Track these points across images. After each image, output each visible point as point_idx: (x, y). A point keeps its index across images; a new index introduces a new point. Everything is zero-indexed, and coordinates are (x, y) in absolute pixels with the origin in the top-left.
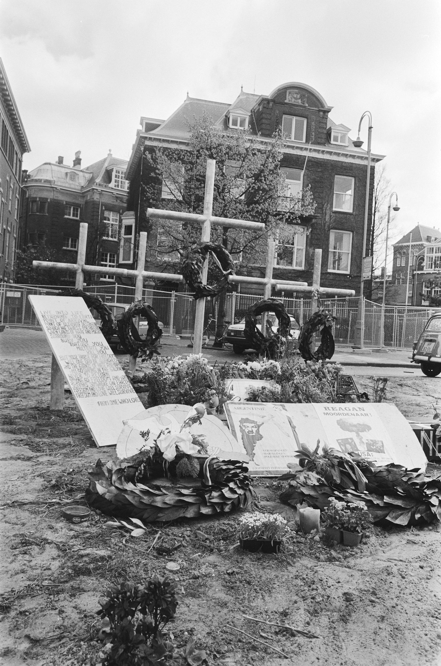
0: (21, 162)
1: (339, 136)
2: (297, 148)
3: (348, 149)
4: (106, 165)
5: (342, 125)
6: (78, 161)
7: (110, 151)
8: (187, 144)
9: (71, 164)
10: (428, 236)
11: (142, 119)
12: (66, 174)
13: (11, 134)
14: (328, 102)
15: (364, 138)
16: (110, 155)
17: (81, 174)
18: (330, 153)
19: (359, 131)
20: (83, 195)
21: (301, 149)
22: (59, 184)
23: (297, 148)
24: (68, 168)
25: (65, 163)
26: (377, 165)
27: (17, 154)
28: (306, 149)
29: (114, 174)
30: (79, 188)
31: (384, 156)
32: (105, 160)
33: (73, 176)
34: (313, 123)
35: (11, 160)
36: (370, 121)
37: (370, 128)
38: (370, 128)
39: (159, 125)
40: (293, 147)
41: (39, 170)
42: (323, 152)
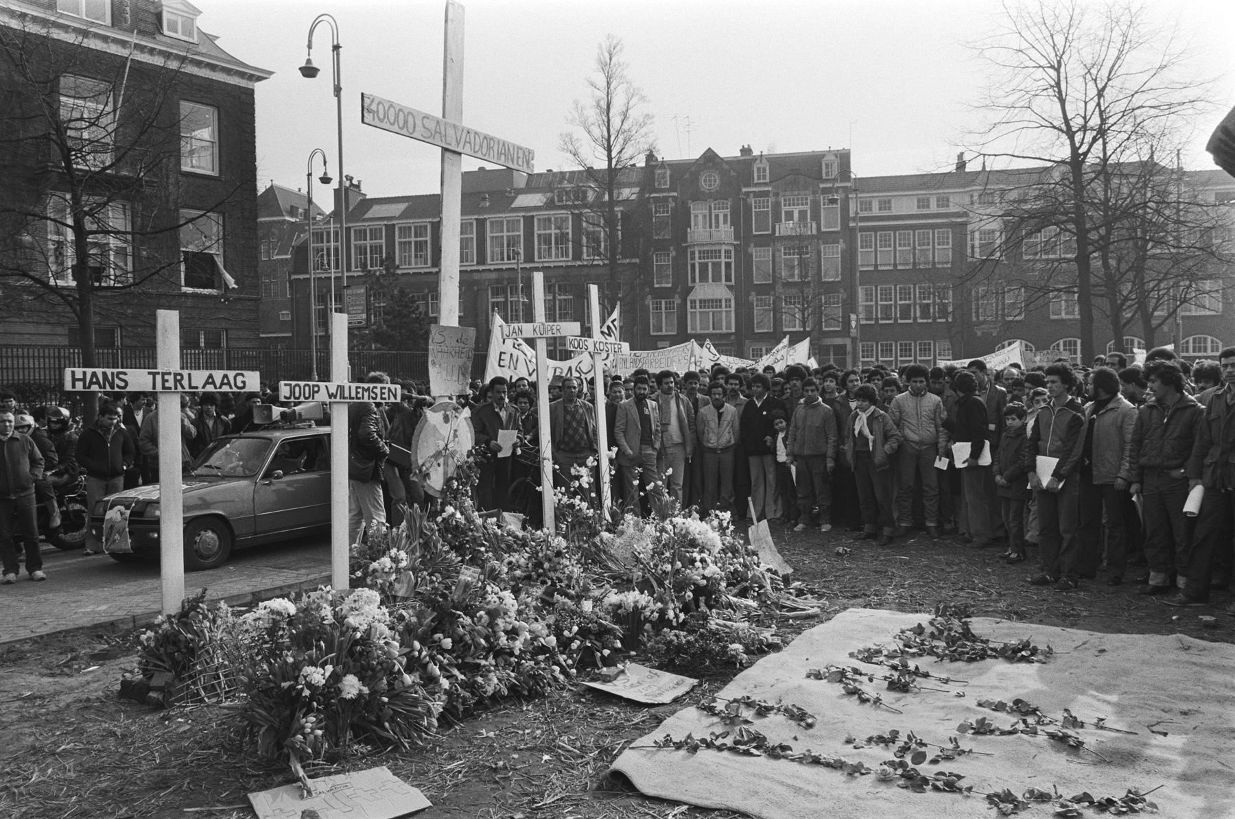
10: (292, 207)
15: (323, 60)
19: (310, 47)
26: (259, 87)
31: (271, 73)
36: (336, 33)
37: (336, 48)
38: (336, 48)
42: (152, 51)
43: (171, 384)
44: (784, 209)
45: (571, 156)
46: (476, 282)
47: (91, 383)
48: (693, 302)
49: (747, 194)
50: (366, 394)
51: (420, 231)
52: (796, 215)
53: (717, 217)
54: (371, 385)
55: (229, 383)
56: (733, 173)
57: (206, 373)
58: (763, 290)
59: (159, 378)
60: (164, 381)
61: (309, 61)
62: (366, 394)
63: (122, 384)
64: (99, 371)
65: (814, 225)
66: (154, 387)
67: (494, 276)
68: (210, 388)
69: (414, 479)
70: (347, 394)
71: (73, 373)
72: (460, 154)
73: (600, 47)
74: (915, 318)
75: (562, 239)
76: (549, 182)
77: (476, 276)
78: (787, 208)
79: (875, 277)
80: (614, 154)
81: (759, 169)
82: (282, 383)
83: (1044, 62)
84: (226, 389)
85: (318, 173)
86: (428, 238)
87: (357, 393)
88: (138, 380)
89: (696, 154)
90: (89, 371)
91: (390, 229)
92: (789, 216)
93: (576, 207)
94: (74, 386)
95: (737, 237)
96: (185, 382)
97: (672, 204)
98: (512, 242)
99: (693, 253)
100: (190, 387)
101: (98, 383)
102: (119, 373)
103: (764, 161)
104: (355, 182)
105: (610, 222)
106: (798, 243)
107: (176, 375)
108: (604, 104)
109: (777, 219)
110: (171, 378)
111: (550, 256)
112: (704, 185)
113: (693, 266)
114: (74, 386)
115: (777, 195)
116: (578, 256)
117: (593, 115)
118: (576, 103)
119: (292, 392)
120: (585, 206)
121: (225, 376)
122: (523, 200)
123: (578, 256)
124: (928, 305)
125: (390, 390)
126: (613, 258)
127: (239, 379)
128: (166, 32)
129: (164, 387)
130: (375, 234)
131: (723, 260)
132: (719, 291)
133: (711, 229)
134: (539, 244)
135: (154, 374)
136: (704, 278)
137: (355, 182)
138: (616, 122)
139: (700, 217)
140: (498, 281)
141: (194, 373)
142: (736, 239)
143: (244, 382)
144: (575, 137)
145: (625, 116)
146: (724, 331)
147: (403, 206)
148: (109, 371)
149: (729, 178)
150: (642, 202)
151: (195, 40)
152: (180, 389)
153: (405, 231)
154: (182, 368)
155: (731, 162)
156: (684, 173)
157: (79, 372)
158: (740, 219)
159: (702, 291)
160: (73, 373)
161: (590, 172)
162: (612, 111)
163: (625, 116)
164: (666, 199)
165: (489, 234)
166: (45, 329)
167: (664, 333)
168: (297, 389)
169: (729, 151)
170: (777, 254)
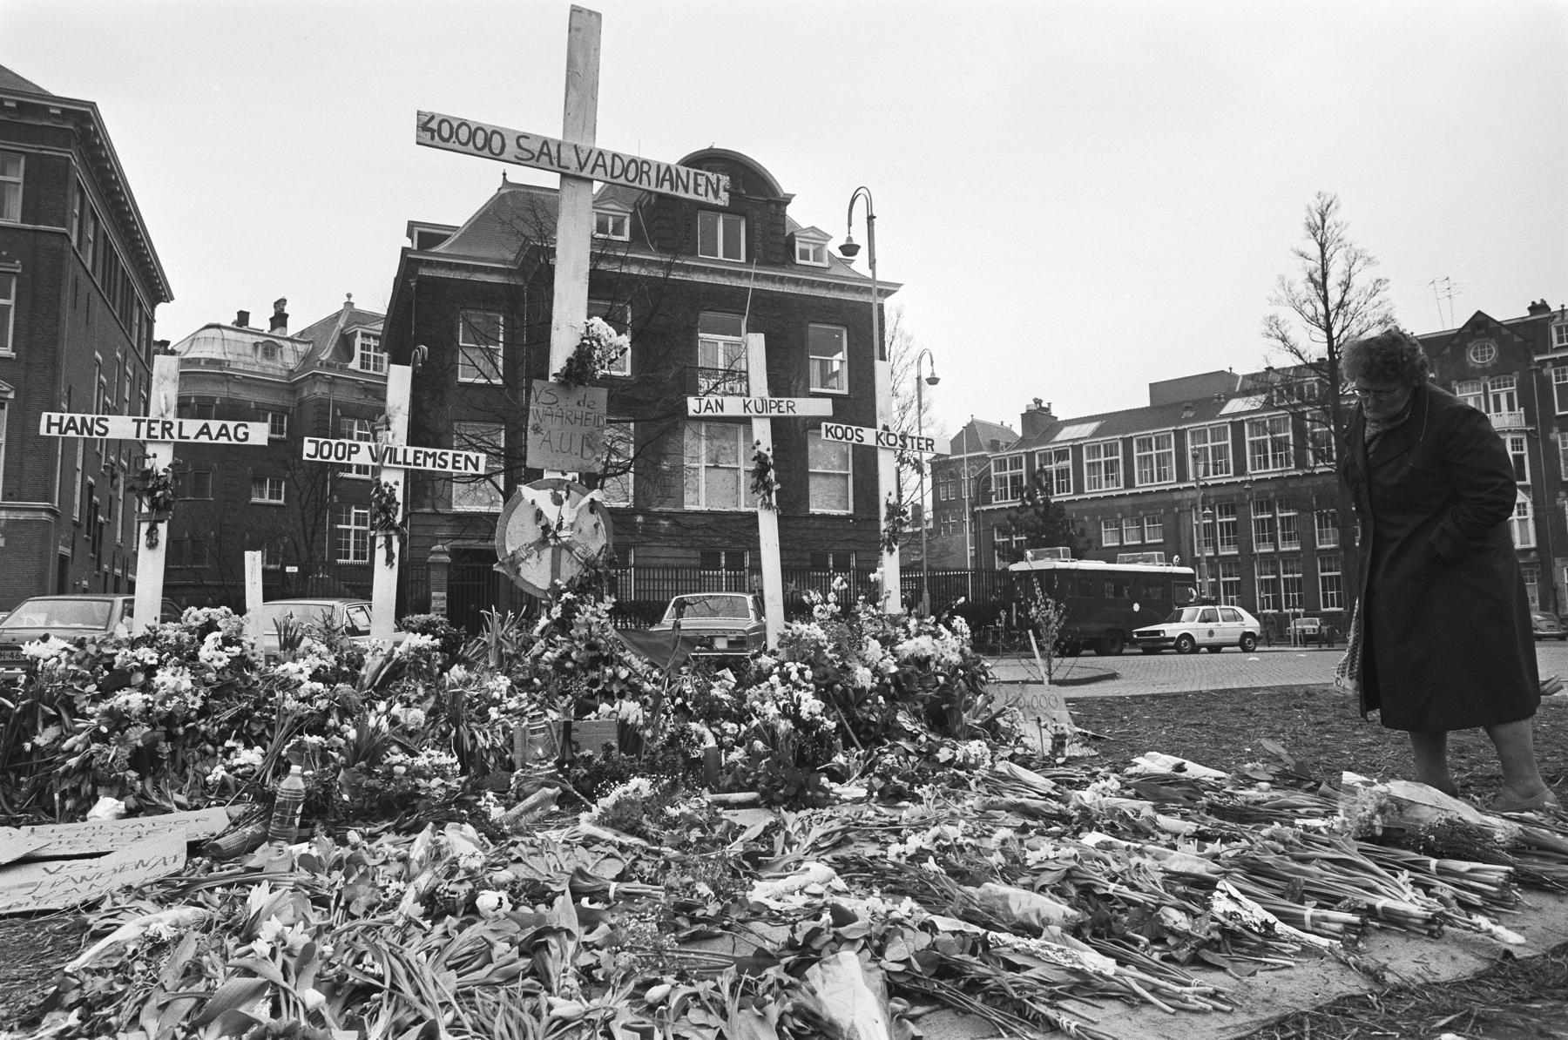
0: (150, 322)
1: (811, 248)
2: (731, 273)
3: (831, 272)
4: (341, 324)
5: (813, 229)
6: (280, 319)
7: (349, 296)
8: (509, 273)
9: (267, 327)
11: (412, 225)
12: (256, 345)
13: (123, 261)
14: (785, 185)
15: (860, 238)
16: (349, 304)
17: (287, 345)
18: (797, 282)
20: (293, 388)
21: (739, 275)
22: (241, 366)
23: (731, 273)
24: (259, 333)
25: (253, 323)
26: (888, 303)
27: (140, 305)
28: (748, 275)
29: (358, 341)
30: (284, 373)
31: (899, 285)
32: (338, 315)
33: (269, 349)
34: (758, 226)
35: (127, 317)
37: (871, 218)
38: (871, 218)
39: (447, 237)
40: (722, 273)
41: (193, 339)
42: (782, 280)
43: (157, 431)
45: (1280, 343)
46: (1177, 503)
47: (68, 428)
50: (430, 461)
51: (1111, 450)
53: (1497, 398)
54: (439, 451)
56: (1517, 339)
57: (201, 423)
59: (144, 426)
60: (150, 429)
61: (850, 239)
62: (430, 461)
64: (78, 417)
68: (204, 439)
69: (500, 569)
70: (400, 458)
72: (591, 181)
73: (1309, 209)
77: (1177, 496)
80: (1335, 333)
84: (223, 440)
85: (926, 375)
86: (1120, 457)
87: (416, 458)
88: (121, 427)
89: (1456, 320)
90: (67, 416)
91: (1077, 450)
93: (1295, 406)
95: (1529, 421)
96: (175, 432)
100: (180, 436)
101: (75, 428)
104: (1044, 405)
107: (164, 423)
108: (1318, 276)
110: (158, 427)
111: (1267, 466)
112: (1473, 360)
117: (1305, 290)
118: (1282, 279)
119: (319, 450)
121: (224, 426)
122: (1235, 405)
125: (467, 458)
128: (798, 261)
129: (149, 435)
130: (1062, 455)
134: (1252, 453)
135: (139, 422)
137: (1044, 405)
138: (1335, 296)
142: (1528, 423)
143: (246, 434)
144: (1281, 319)
145: (1346, 285)
147: (1095, 425)
148: (88, 417)
151: (825, 264)
152: (167, 438)
153: (1094, 450)
157: (55, 417)
166: (679, 552)
168: (326, 447)
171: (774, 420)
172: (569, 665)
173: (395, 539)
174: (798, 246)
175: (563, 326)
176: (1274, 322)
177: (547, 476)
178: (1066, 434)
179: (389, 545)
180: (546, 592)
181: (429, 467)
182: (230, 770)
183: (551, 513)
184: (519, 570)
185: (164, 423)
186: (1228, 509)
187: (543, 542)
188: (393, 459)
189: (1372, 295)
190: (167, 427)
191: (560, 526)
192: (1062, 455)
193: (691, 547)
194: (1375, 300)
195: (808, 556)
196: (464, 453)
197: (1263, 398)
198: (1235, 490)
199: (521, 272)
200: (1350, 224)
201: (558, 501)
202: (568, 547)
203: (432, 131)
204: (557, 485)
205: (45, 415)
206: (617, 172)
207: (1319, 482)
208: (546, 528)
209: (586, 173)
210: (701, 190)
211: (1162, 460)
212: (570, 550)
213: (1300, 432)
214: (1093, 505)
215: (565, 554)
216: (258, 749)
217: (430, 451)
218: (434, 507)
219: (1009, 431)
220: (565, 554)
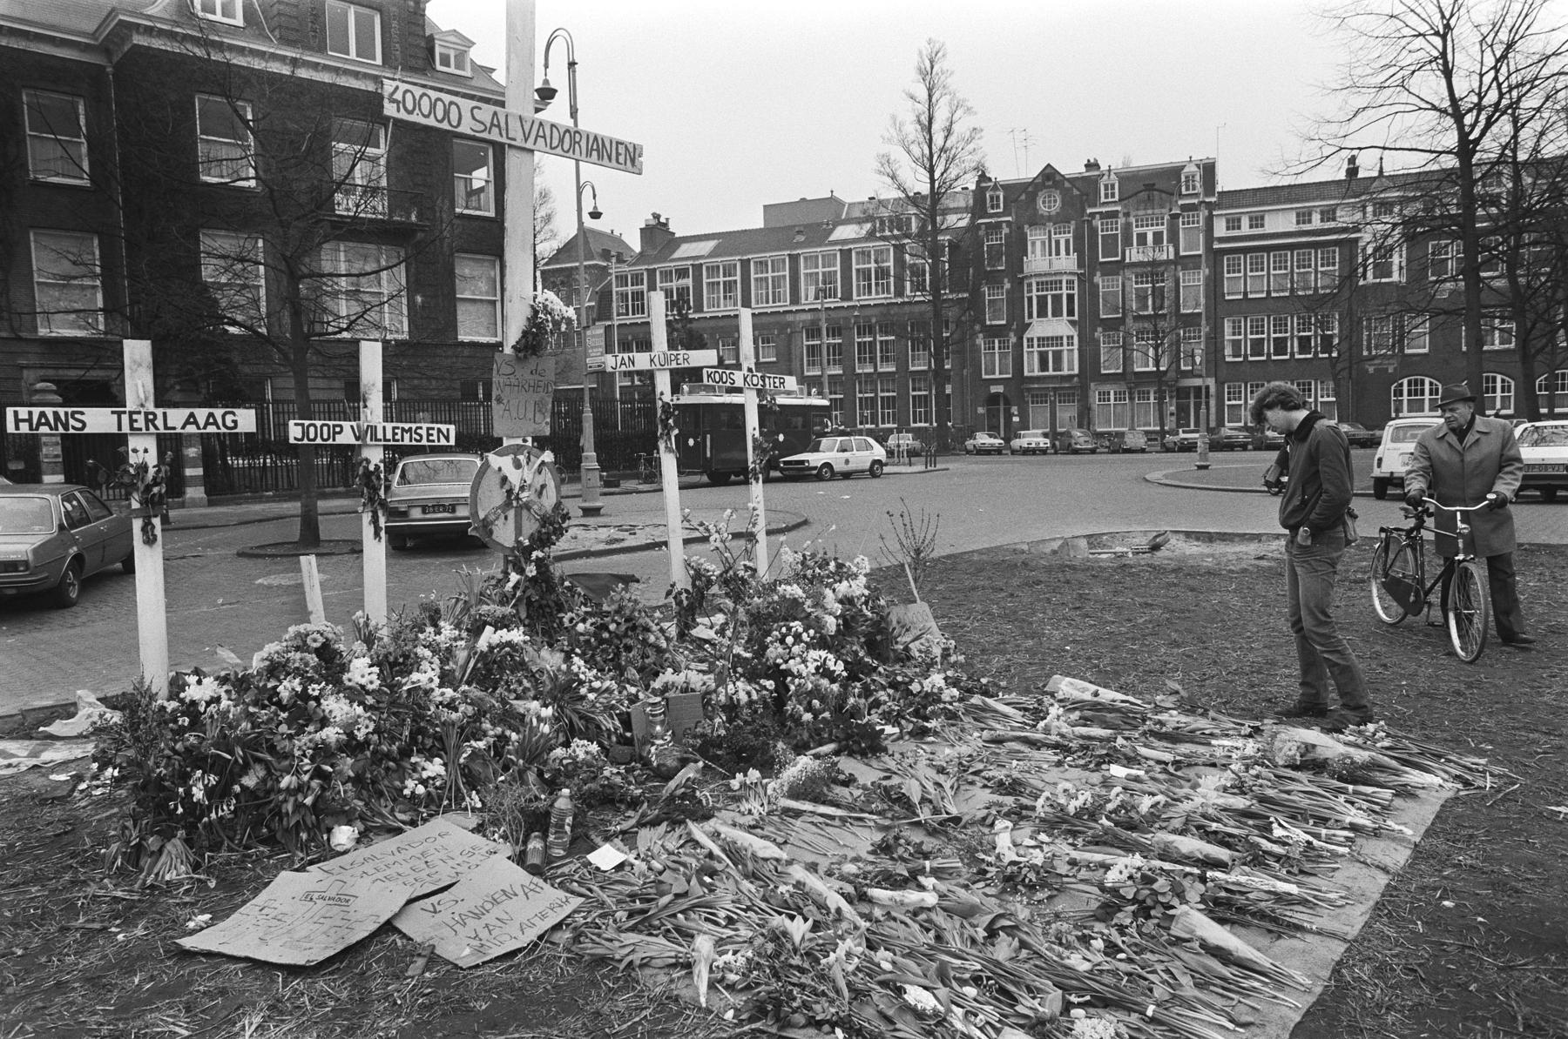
1: (452, 54)
3: (473, 83)
15: (559, 81)
19: (546, 66)
34: (395, 24)
36: (570, 49)
37: (572, 64)
38: (572, 64)
43: (141, 423)
44: (1136, 231)
45: (889, 180)
46: (789, 324)
47: (39, 424)
48: (1030, 340)
49: (1093, 215)
50: (407, 436)
51: (729, 271)
52: (1150, 237)
53: (1058, 243)
54: (414, 426)
55: (215, 423)
56: (1076, 192)
57: (186, 412)
58: (1111, 325)
59: (125, 418)
60: (132, 421)
61: (546, 82)
62: (407, 436)
63: (79, 425)
64: (49, 411)
65: (1171, 249)
66: (120, 428)
67: (808, 317)
68: (191, 429)
70: (380, 436)
71: (16, 413)
72: (532, 151)
73: (920, 53)
74: (1292, 354)
75: (882, 273)
76: (869, 213)
77: (790, 318)
78: (1140, 230)
79: (1247, 306)
80: (937, 175)
81: (1106, 187)
82: (291, 423)
83: (1424, 28)
84: (212, 429)
86: (738, 278)
87: (394, 434)
89: (1031, 172)
90: (36, 411)
91: (698, 268)
92: (1142, 239)
93: (895, 237)
94: (17, 428)
95: (1080, 266)
96: (160, 422)
97: (1005, 230)
98: (829, 279)
99: (1030, 285)
100: (166, 427)
101: (47, 423)
102: (73, 413)
103: (1113, 176)
104: (662, 220)
105: (935, 251)
106: (1152, 270)
107: (146, 414)
109: (1127, 242)
110: (141, 419)
111: (870, 293)
112: (1043, 208)
113: (1030, 299)
114: (17, 428)
115: (1127, 215)
116: (900, 292)
117: (913, 131)
118: (894, 118)
119: (305, 433)
120: (908, 236)
121: (211, 415)
122: (844, 232)
123: (900, 292)
124: (1309, 338)
125: (439, 431)
126: (935, 290)
127: (229, 418)
128: (439, 67)
129: (132, 428)
130: (682, 273)
131: (1065, 292)
132: (1059, 327)
133: (1052, 257)
135: (119, 414)
136: (1042, 313)
137: (662, 220)
138: (938, 140)
139: (1038, 244)
140: (815, 322)
141: (170, 412)
143: (235, 422)
145: (949, 132)
146: (1065, 372)
147: (712, 244)
148: (61, 411)
149: (1071, 196)
150: (972, 228)
151: (468, 73)
152: (152, 429)
153: (713, 270)
154: (157, 406)
155: (1073, 181)
156: (1022, 195)
157: (23, 412)
158: (1084, 246)
159: (1040, 328)
160: (16, 413)
161: (915, 200)
162: (935, 127)
163: (949, 132)
164: (998, 225)
165: (803, 271)
167: (997, 376)
168: (312, 429)
169: (1071, 167)
170: (1128, 283)
171: (671, 371)
172: (606, 635)
173: (380, 513)
174: (438, 50)
175: (516, 299)
176: (887, 160)
177: (506, 443)
178: (685, 250)
179: (375, 521)
180: (512, 549)
181: (407, 442)
182: (424, 782)
183: (515, 477)
184: (491, 532)
185: (146, 414)
186: (834, 331)
187: (507, 505)
188: (374, 437)
189: (968, 142)
190: (150, 420)
191: (522, 488)
192: (682, 273)
193: (336, 377)
194: (971, 147)
195: (457, 385)
196: (436, 426)
197: (868, 226)
198: (843, 314)
199: (105, 49)
200: (958, 77)
201: (518, 465)
202: (527, 506)
203: (398, 102)
204: (517, 450)
205: (10, 411)
206: (555, 143)
207: (917, 309)
208: (510, 492)
209: (529, 145)
210: (621, 159)
211: (777, 282)
212: (529, 509)
213: (900, 262)
214: (712, 323)
215: (525, 512)
216: (437, 760)
217: (407, 426)
218: (12, 329)
219: (619, 241)
220: (525, 512)
